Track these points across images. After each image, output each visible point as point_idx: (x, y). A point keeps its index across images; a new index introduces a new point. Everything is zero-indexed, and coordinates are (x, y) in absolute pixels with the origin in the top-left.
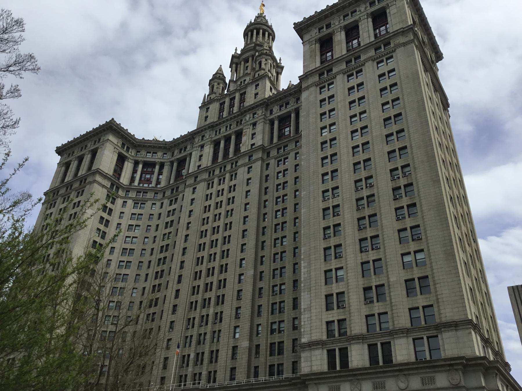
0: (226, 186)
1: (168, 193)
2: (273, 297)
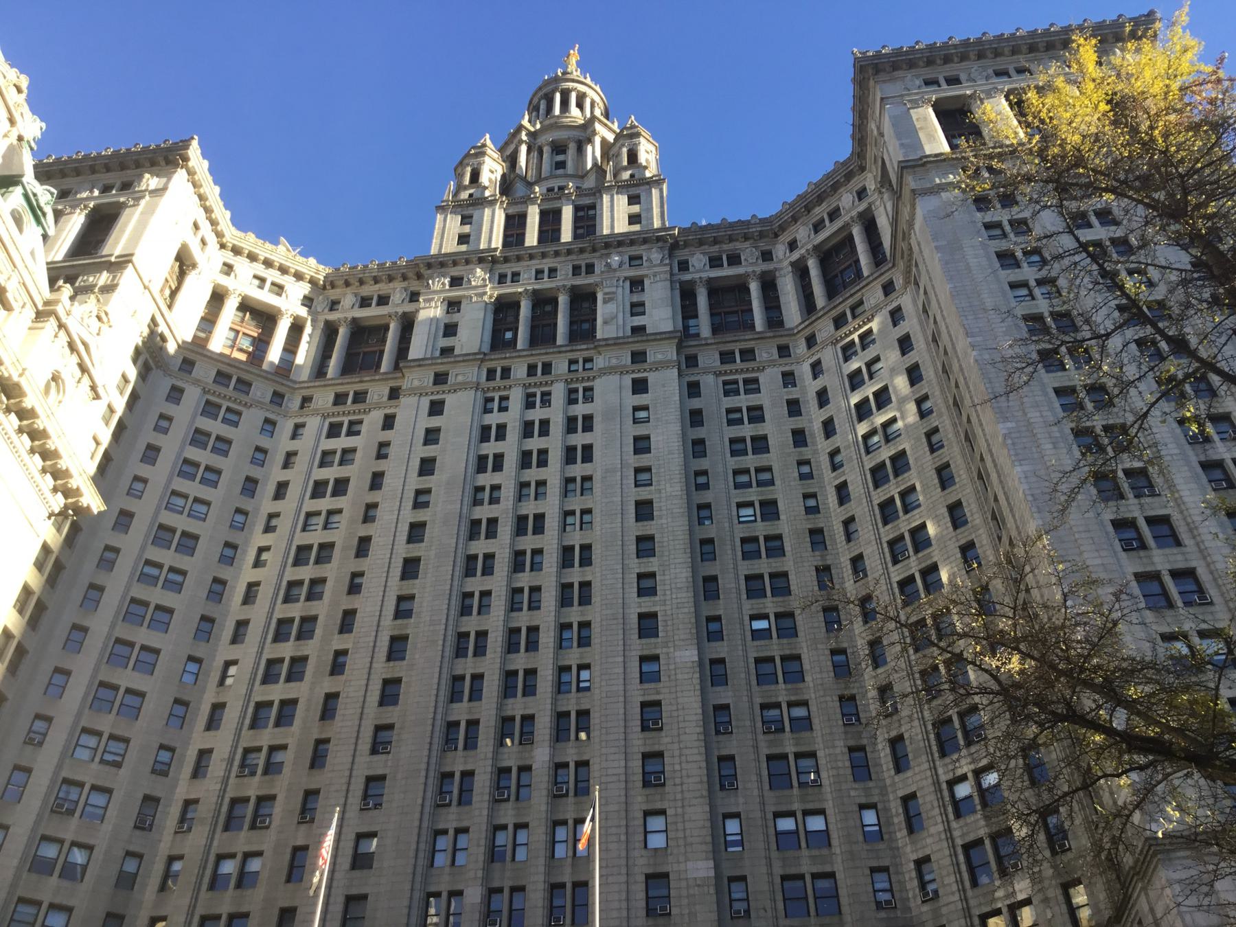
0: (556, 413)
1: (323, 399)
2: (771, 737)
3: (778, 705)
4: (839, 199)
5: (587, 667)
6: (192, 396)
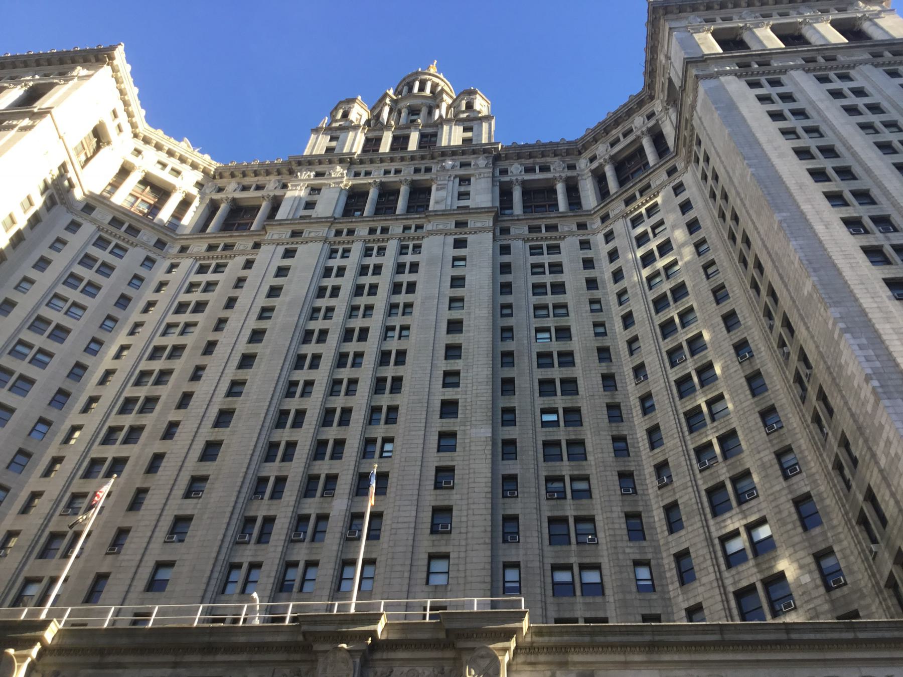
1: (199, 247)
3: (561, 479)
4: (633, 122)
5: (390, 440)
6: (88, 230)
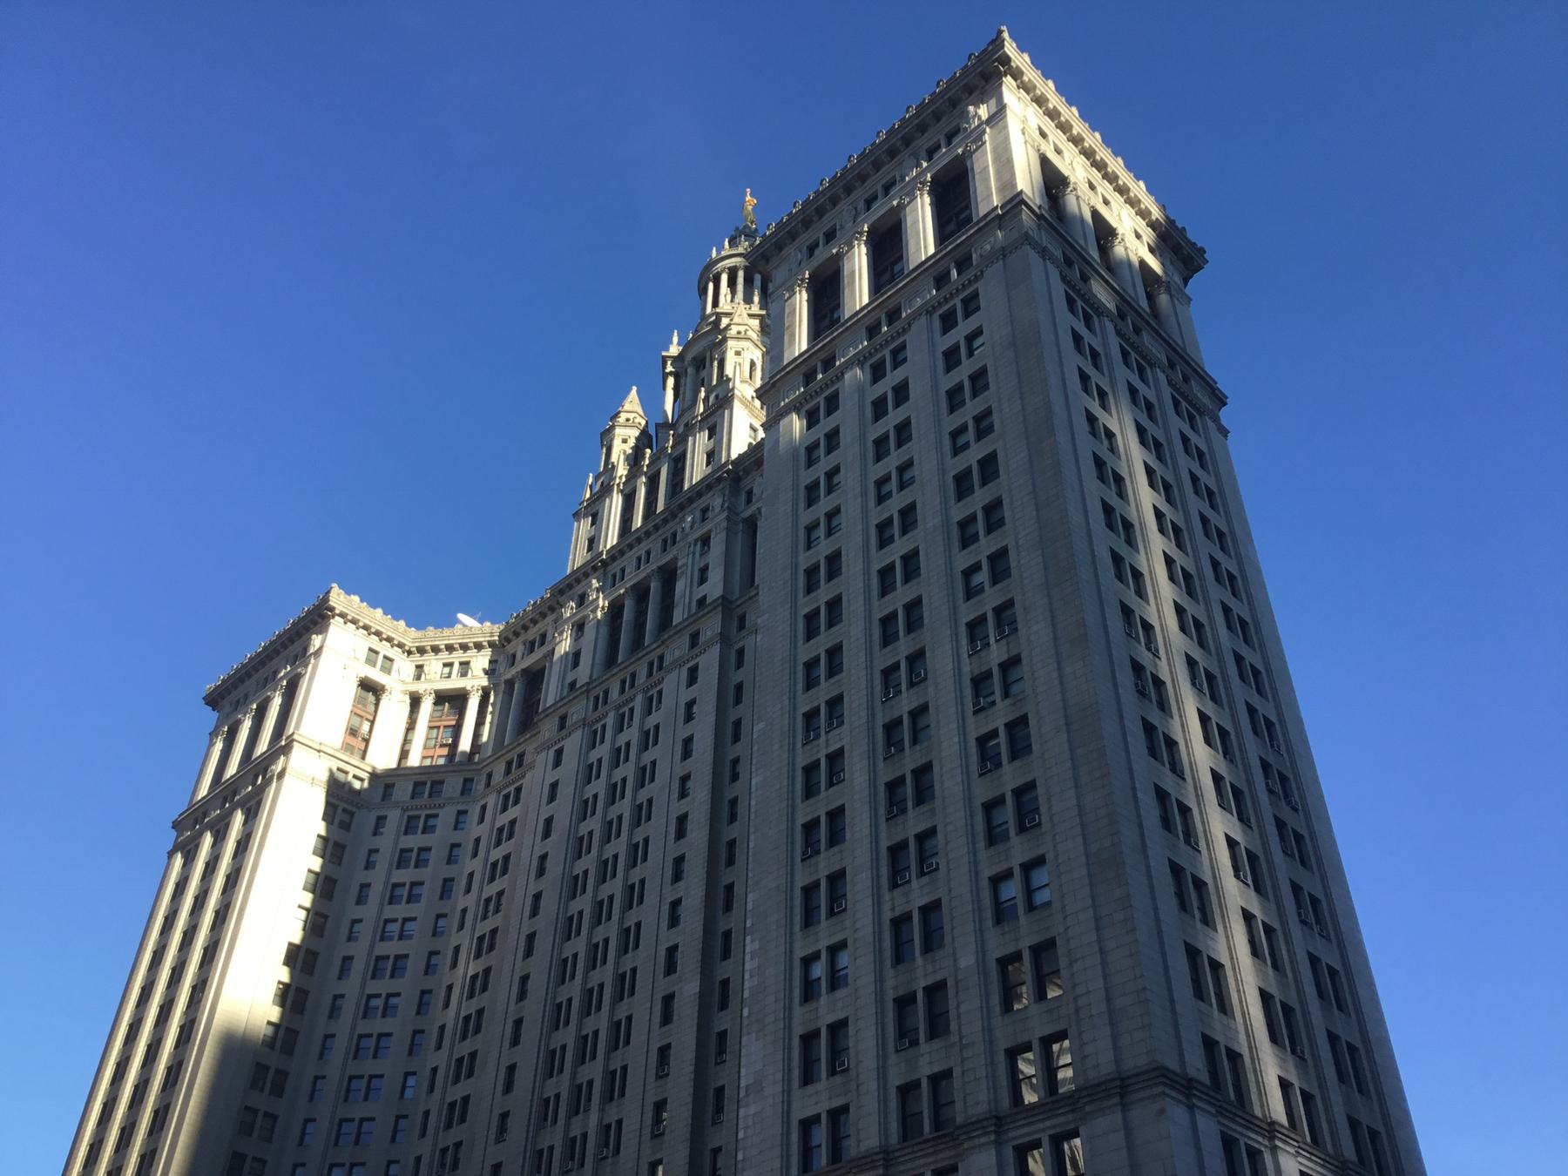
0: (632, 734)
